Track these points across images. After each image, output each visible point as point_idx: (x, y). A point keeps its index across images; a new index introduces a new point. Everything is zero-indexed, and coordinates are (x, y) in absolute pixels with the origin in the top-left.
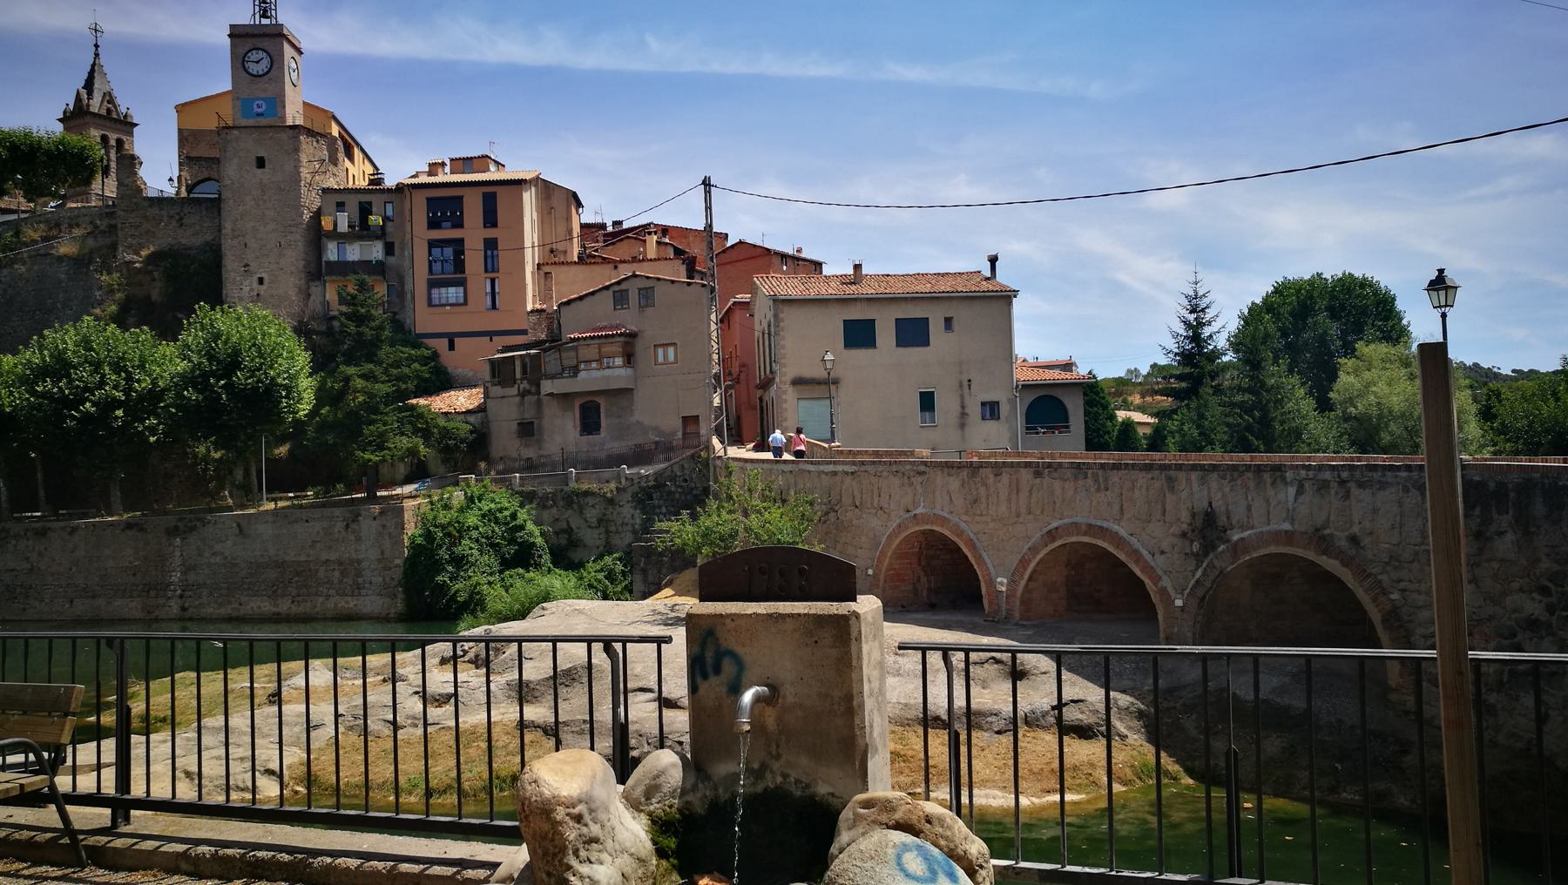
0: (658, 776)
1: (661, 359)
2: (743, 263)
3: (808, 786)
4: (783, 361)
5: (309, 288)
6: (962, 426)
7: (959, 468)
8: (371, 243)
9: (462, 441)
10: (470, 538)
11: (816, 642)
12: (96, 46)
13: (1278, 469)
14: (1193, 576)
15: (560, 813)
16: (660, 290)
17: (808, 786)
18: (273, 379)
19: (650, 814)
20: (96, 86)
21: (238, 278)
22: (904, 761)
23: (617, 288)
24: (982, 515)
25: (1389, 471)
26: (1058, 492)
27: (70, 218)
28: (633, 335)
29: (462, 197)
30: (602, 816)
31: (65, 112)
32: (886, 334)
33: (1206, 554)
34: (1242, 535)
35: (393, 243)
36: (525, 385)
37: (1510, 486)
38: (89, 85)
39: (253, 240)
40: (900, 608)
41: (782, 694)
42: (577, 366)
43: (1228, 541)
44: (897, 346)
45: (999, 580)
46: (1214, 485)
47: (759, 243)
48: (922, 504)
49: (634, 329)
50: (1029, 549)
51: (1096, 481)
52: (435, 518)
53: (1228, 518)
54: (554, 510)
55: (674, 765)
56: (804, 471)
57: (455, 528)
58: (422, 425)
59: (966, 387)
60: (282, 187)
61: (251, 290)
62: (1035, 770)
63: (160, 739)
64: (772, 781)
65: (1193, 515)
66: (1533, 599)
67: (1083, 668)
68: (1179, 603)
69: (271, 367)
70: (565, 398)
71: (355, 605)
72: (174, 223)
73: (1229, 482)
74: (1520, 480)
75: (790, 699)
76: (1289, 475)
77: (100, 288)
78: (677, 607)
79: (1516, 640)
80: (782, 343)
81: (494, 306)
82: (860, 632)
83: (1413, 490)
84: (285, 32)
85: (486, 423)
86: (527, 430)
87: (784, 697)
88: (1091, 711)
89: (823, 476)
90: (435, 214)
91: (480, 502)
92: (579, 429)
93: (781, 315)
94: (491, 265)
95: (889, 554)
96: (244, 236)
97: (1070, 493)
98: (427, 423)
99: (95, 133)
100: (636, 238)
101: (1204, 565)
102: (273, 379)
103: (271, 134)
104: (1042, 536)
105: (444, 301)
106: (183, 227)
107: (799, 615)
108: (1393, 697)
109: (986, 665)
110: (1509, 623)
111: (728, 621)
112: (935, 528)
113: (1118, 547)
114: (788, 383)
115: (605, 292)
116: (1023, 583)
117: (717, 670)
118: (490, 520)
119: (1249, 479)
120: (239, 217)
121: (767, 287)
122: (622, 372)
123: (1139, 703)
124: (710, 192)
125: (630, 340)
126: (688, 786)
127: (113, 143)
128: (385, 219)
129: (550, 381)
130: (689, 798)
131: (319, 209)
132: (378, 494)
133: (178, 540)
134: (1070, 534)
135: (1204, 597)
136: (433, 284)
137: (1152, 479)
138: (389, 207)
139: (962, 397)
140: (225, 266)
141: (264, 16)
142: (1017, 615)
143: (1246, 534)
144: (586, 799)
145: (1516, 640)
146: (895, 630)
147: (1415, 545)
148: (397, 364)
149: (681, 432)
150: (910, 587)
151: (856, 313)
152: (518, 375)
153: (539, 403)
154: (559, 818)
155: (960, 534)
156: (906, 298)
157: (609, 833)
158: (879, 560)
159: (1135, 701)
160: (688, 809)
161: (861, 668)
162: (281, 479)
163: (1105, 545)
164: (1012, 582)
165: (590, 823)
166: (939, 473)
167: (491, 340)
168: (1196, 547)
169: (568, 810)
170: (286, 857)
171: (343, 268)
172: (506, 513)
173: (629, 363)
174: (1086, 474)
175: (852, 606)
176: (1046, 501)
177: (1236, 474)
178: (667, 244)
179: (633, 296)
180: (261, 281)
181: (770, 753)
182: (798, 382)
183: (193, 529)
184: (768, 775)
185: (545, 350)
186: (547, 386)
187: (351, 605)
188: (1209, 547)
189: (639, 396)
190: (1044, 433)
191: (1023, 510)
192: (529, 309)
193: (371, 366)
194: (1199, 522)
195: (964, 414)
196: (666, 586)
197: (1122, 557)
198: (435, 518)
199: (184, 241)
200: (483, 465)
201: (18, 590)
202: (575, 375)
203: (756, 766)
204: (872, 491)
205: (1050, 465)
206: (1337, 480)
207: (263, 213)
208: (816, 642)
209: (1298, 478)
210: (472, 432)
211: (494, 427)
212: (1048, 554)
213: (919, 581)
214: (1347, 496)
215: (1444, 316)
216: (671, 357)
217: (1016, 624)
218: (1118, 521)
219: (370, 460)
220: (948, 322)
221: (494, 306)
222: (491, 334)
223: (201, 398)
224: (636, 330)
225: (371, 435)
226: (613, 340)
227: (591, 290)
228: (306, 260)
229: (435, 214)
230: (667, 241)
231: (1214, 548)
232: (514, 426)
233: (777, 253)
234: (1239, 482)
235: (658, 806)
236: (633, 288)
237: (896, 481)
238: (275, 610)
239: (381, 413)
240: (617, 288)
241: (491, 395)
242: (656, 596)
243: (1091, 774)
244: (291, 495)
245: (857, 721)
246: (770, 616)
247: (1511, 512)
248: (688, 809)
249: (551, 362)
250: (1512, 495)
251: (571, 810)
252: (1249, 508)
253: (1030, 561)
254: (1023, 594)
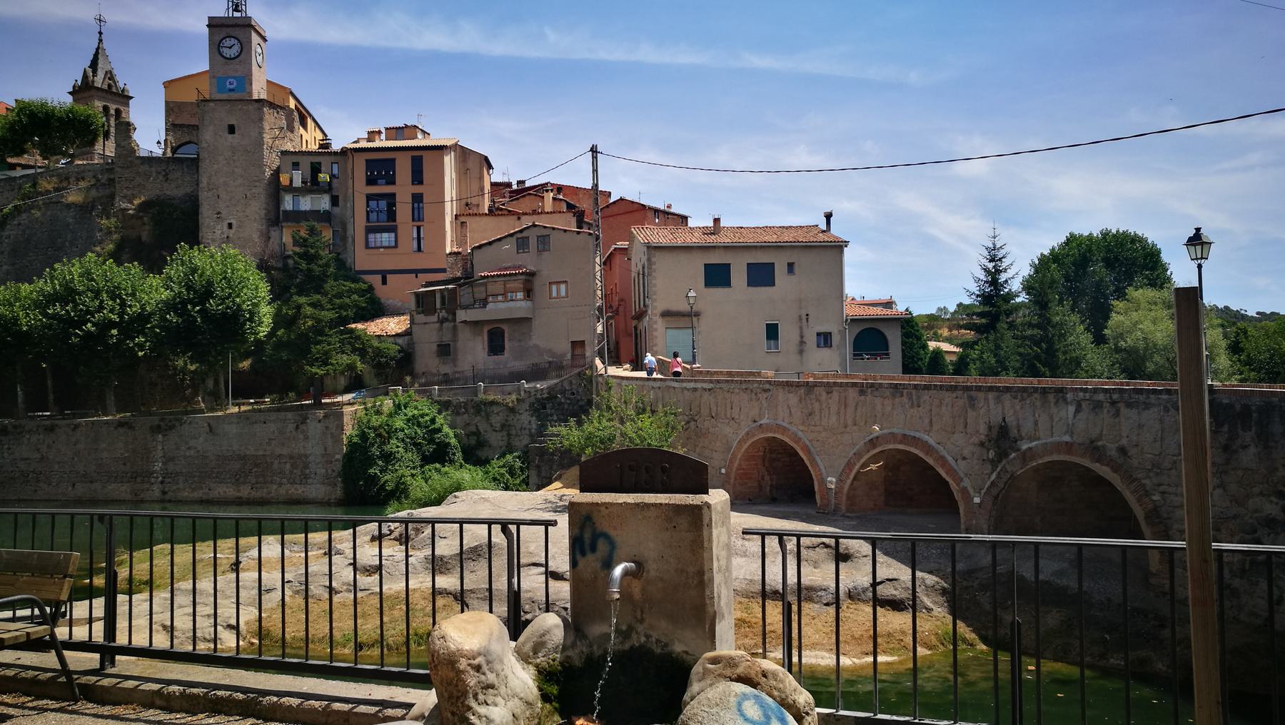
0: (544, 635)
1: (554, 294)
2: (623, 216)
3: (666, 645)
4: (654, 297)
5: (269, 232)
6: (801, 352)
7: (797, 386)
8: (320, 196)
9: (392, 359)
10: (397, 438)
11: (675, 527)
12: (100, 33)
13: (1060, 391)
14: (989, 478)
15: (463, 664)
16: (554, 236)
17: (666, 645)
18: (239, 306)
19: (537, 666)
20: (100, 65)
21: (212, 224)
22: (749, 627)
23: (519, 235)
24: (815, 426)
25: (1153, 394)
26: (879, 407)
27: (78, 173)
28: (532, 274)
29: (394, 160)
30: (498, 667)
31: (74, 87)
32: (739, 276)
33: (1000, 461)
34: (1030, 445)
35: (337, 197)
36: (443, 314)
37: (1253, 408)
38: (94, 64)
39: (224, 193)
40: (748, 502)
41: (646, 569)
42: (486, 299)
43: (1019, 450)
44: (748, 286)
45: (829, 479)
46: (1007, 404)
47: (636, 200)
48: (767, 416)
49: (533, 269)
50: (855, 454)
51: (910, 398)
52: (369, 421)
53: (1019, 431)
54: (466, 416)
55: (557, 626)
56: (670, 387)
57: (385, 430)
58: (360, 345)
59: (804, 320)
60: (249, 150)
61: (222, 233)
62: (857, 636)
63: (140, 599)
64: (637, 640)
65: (990, 428)
66: (1271, 502)
67: (897, 552)
68: (977, 500)
69: (238, 296)
70: (476, 324)
71: (303, 492)
72: (161, 177)
73: (1020, 401)
74: (1262, 403)
75: (653, 574)
76: (1069, 396)
77: (101, 230)
78: (565, 498)
79: (1256, 535)
80: (654, 282)
81: (419, 249)
82: (711, 519)
83: (1173, 410)
84: (253, 23)
85: (411, 344)
86: (445, 350)
87: (648, 571)
88: (902, 588)
89: (686, 392)
90: (372, 173)
91: (405, 408)
92: (487, 350)
93: (653, 259)
94: (417, 216)
95: (739, 457)
96: (217, 189)
97: (889, 408)
98: (363, 344)
99: (99, 104)
100: (536, 195)
101: (998, 469)
102: (239, 306)
103: (240, 107)
104: (865, 443)
105: (378, 244)
106: (169, 182)
107: (661, 504)
108: (1153, 581)
109: (817, 549)
110: (1251, 521)
111: (603, 508)
112: (776, 435)
113: (927, 454)
114: (658, 315)
115: (509, 239)
116: (849, 482)
117: (593, 549)
118: (413, 424)
119: (1036, 399)
120: (213, 173)
121: (642, 236)
122: (523, 304)
123: (942, 581)
124: (596, 158)
125: (530, 278)
126: (569, 643)
127: (112, 112)
128: (332, 176)
129: (464, 311)
130: (570, 653)
131: (278, 168)
132: (323, 401)
133: (160, 436)
134: (888, 442)
135: (998, 495)
136: (369, 230)
137: (957, 398)
138: (335, 166)
139: (801, 328)
140: (202, 213)
141: (236, 10)
142: (843, 508)
143: (1034, 443)
144: (484, 653)
145: (1256, 535)
146: (743, 519)
147: (1175, 456)
148: (340, 296)
149: (570, 354)
150: (756, 484)
151: (715, 259)
152: (438, 305)
153: (455, 328)
154: (461, 668)
155: (798, 440)
156: (756, 247)
157: (503, 680)
158: (731, 462)
159: (940, 580)
160: (568, 663)
161: (712, 549)
162: (244, 389)
163: (916, 451)
164: (840, 481)
165: (488, 672)
166: (781, 390)
167: (417, 277)
168: (992, 454)
169: (469, 661)
170: (240, 696)
171: (297, 216)
172: (427, 418)
173: (529, 296)
174: (903, 393)
175: (705, 498)
176: (869, 415)
177: (1025, 395)
178: (561, 200)
179: (533, 242)
180: (230, 226)
181: (636, 618)
182: (666, 314)
183: (172, 428)
184: (634, 636)
185: (460, 286)
186: (462, 315)
187: (300, 492)
188: (1002, 455)
189: (535, 323)
190: (868, 359)
191: (850, 422)
192: (448, 252)
193: (319, 296)
194: (994, 434)
195: (802, 343)
196: (556, 480)
197: (931, 461)
198: (369, 421)
199: (168, 193)
200: (408, 379)
201: (30, 476)
202: (485, 306)
203: (624, 628)
204: (726, 404)
205: (872, 385)
206: (1109, 401)
207: (233, 171)
208: (675, 527)
209: (1076, 399)
210: (400, 352)
211: (417, 347)
212: (869, 459)
213: (763, 479)
214: (1117, 414)
215: (1200, 267)
216: (563, 293)
217: (843, 516)
218: (928, 432)
219: (316, 374)
220: (791, 266)
221: (419, 249)
222: (416, 272)
223: (180, 320)
224: (535, 270)
225: (318, 353)
226: (515, 278)
227: (499, 237)
228: (266, 209)
229: (372, 173)
230: (561, 197)
231: (1007, 455)
232: (434, 347)
233: (650, 208)
234: (1028, 402)
235: (543, 659)
236: (533, 236)
237: (745, 396)
238: (238, 494)
239: (326, 335)
240: (519, 235)
241: (416, 321)
242: (548, 488)
243: (902, 640)
244: (252, 401)
245: (708, 592)
246: (637, 505)
247: (1253, 429)
248: (568, 663)
249: (465, 295)
250: (1255, 415)
251: (472, 662)
252: (1036, 423)
253: (855, 464)
254: (849, 491)
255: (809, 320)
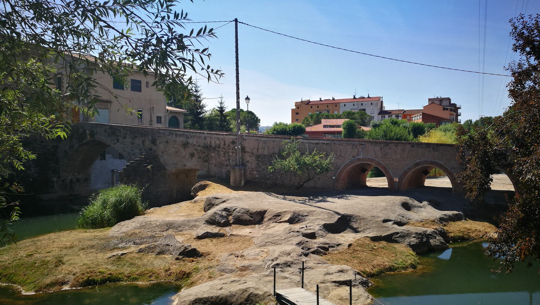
7: (380, 143)
48: (362, 155)
59: (152, 110)
89: (311, 144)
104: (414, 165)
164: (401, 179)
195: (151, 121)
255: (154, 110)
